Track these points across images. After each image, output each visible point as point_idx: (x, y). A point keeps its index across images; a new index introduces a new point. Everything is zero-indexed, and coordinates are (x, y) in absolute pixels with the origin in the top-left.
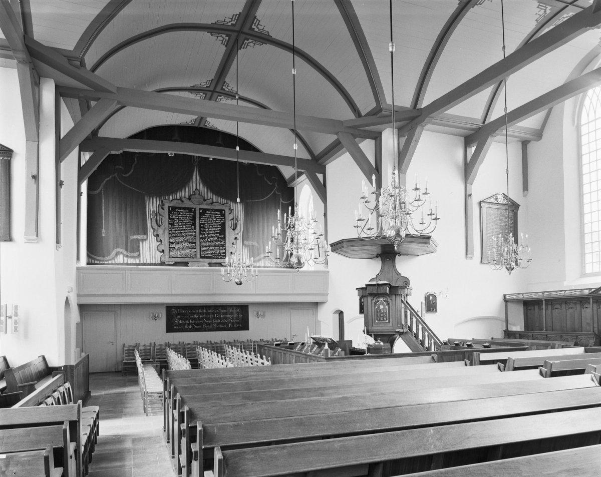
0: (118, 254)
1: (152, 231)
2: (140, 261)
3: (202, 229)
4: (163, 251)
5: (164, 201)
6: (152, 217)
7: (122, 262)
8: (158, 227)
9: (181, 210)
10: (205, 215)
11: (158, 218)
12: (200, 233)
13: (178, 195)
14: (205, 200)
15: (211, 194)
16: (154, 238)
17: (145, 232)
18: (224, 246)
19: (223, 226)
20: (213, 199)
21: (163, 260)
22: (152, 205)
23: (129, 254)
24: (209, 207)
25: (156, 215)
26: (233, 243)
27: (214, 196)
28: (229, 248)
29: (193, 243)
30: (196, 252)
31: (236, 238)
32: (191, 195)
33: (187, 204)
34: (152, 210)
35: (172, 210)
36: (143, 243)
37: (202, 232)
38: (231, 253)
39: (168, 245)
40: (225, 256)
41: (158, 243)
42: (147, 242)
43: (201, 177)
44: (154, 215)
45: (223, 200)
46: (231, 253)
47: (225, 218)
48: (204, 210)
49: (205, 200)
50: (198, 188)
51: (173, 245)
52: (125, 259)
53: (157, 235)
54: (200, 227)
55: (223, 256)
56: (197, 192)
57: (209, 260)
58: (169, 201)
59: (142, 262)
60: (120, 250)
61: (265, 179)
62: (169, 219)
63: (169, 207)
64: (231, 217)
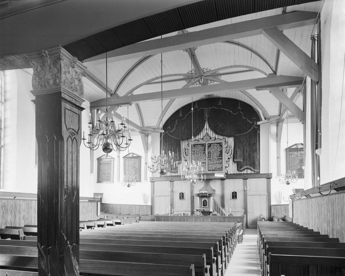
2: (178, 174)
3: (209, 155)
6: (184, 151)
8: (186, 156)
9: (198, 146)
10: (210, 147)
12: (208, 157)
15: (215, 134)
17: (180, 159)
18: (221, 163)
19: (221, 152)
20: (215, 137)
22: (184, 145)
24: (213, 142)
25: (185, 150)
26: (227, 161)
27: (217, 135)
28: (225, 164)
29: (204, 163)
30: (205, 168)
31: (229, 158)
32: (203, 137)
33: (201, 142)
34: (184, 147)
37: (209, 157)
38: (226, 167)
40: (222, 169)
42: (181, 164)
43: (209, 126)
44: (184, 150)
45: (222, 137)
46: (226, 167)
47: (222, 148)
54: (208, 154)
55: (221, 169)
59: (178, 175)
61: (248, 120)
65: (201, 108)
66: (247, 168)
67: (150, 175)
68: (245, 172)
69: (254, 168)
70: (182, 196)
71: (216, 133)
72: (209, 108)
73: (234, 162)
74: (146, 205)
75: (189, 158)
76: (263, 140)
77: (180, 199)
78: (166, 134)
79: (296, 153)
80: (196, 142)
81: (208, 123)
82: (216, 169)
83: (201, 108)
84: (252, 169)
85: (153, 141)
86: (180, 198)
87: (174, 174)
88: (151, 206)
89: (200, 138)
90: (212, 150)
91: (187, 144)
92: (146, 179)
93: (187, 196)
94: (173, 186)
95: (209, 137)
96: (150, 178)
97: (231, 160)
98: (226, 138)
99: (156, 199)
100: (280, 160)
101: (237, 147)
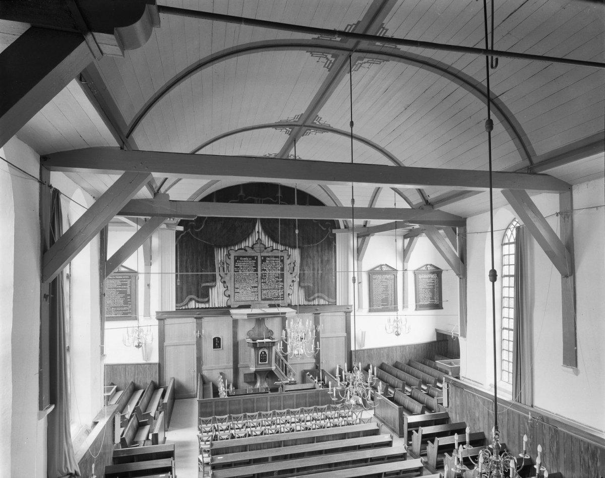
0: (191, 300)
1: (220, 278)
2: (209, 305)
4: (229, 296)
5: (230, 251)
7: (194, 307)
11: (225, 267)
12: (262, 278)
13: (243, 245)
14: (266, 248)
15: (272, 242)
16: (222, 285)
17: (214, 279)
20: (273, 247)
21: (229, 304)
23: (200, 300)
24: (270, 254)
25: (223, 263)
27: (274, 244)
28: (287, 291)
29: (255, 287)
32: (254, 244)
33: (250, 253)
35: (237, 259)
36: (212, 290)
39: (233, 290)
40: (283, 297)
41: (225, 289)
44: (221, 264)
47: (283, 264)
48: (265, 257)
49: (266, 248)
50: (260, 238)
51: (238, 291)
52: (197, 304)
53: (224, 282)
56: (259, 241)
57: (269, 302)
58: (235, 251)
59: (211, 306)
60: (192, 296)
61: (320, 225)
62: (235, 267)
63: (235, 256)
64: (289, 262)
65: (250, 197)
66: (318, 297)
67: (155, 307)
68: (316, 302)
69: (328, 296)
70: (217, 343)
71: (275, 240)
72: (263, 199)
73: (300, 288)
74: (148, 362)
75: (230, 279)
76: (340, 254)
77: (214, 348)
78: (188, 233)
79: (379, 277)
80: (241, 253)
81: (261, 223)
82: (274, 298)
83: (250, 197)
84: (326, 298)
85: (162, 248)
86: (215, 347)
87: (203, 306)
88: (159, 364)
89: (247, 245)
90: (267, 266)
91: (225, 254)
92: (147, 314)
93: (227, 342)
94: (199, 327)
95: (263, 246)
96: (157, 313)
97: (296, 284)
98: (289, 249)
99: (170, 352)
100: (362, 286)
101: (305, 263)
